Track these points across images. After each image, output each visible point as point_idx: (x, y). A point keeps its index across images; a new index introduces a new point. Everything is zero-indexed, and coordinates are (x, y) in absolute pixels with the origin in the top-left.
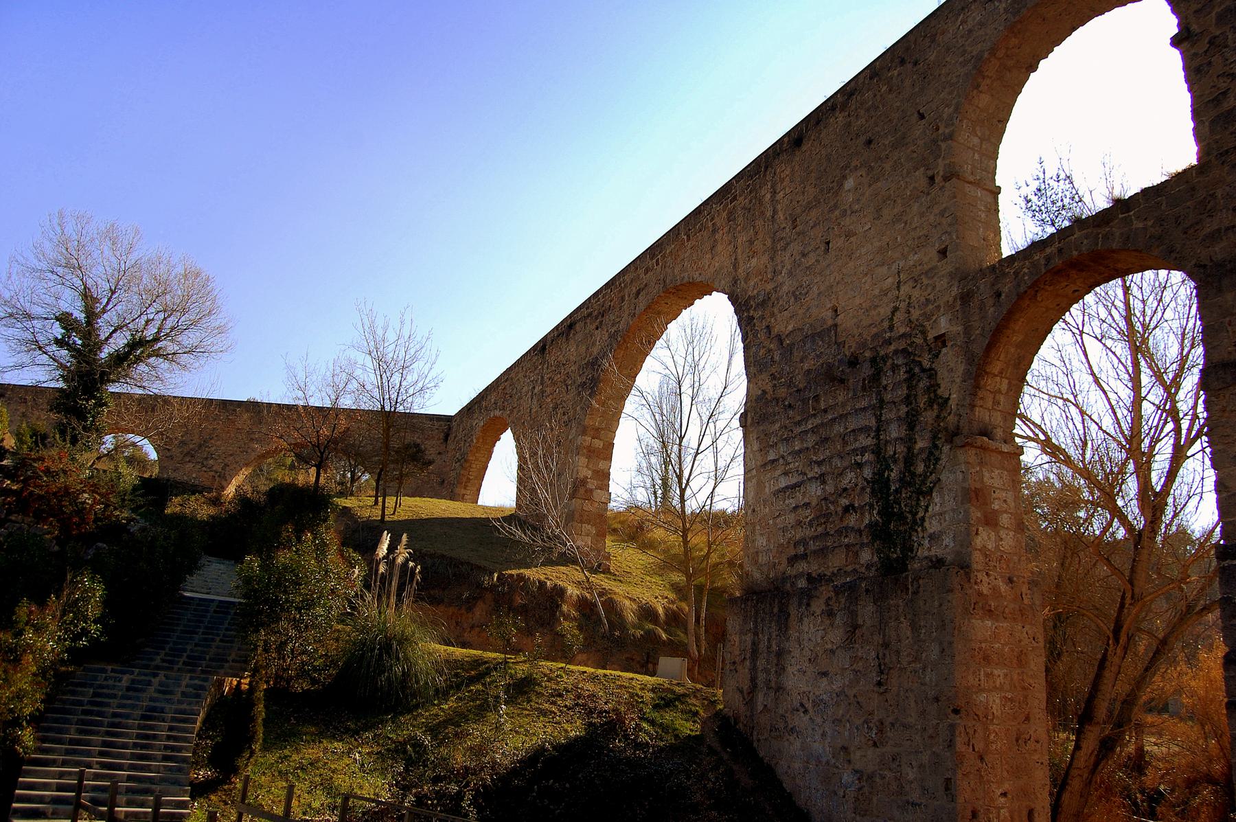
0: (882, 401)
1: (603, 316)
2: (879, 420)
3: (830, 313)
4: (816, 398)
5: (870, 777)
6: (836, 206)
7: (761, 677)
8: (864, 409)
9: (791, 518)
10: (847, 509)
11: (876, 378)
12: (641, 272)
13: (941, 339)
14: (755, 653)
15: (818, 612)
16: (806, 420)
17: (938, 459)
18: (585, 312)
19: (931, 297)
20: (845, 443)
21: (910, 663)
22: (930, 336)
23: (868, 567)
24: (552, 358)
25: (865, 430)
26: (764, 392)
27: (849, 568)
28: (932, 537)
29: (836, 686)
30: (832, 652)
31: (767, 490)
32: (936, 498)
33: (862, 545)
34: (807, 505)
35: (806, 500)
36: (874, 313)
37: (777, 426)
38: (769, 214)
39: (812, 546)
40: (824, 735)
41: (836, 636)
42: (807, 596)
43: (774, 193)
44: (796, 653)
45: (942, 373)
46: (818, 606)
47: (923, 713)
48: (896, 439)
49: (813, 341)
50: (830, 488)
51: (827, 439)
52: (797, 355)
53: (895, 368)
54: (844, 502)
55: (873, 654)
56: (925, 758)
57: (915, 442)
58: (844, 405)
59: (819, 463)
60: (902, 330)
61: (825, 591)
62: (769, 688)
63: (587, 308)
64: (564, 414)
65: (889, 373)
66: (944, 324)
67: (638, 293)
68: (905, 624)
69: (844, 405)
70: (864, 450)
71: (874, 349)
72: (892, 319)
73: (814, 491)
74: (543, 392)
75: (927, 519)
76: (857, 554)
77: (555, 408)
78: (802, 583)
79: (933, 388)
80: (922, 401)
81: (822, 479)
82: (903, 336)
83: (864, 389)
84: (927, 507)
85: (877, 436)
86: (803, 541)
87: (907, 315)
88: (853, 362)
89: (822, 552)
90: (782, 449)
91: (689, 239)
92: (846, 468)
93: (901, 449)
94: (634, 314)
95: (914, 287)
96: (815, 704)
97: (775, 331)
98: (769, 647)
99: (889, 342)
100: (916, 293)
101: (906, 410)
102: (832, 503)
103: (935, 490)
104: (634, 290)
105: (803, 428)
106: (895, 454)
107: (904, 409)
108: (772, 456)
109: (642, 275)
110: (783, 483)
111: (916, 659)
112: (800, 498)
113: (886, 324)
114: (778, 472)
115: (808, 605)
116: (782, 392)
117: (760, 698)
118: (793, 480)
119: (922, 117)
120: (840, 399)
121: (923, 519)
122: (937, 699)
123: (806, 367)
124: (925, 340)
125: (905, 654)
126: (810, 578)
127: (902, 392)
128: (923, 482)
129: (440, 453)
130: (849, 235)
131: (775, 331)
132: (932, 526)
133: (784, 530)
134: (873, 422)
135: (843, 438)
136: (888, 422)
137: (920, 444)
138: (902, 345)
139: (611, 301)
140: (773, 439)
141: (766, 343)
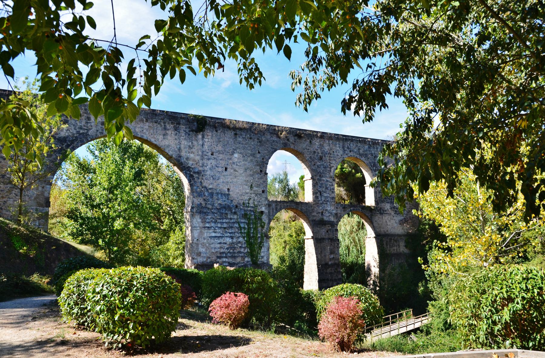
4: (227, 214)
6: (231, 159)
10: (241, 247)
13: (262, 213)
16: (223, 219)
26: (201, 203)
28: (262, 257)
31: (205, 235)
32: (263, 248)
34: (225, 243)
35: (225, 242)
37: (209, 217)
38: (201, 143)
49: (222, 196)
52: (215, 197)
54: (240, 245)
59: (230, 233)
60: (252, 205)
66: (263, 209)
73: (229, 240)
76: (244, 259)
81: (232, 238)
82: (252, 207)
83: (242, 217)
90: (213, 225)
99: (248, 207)
100: (256, 198)
105: (221, 221)
108: (207, 225)
110: (214, 235)
114: (211, 231)
116: (210, 207)
118: (219, 235)
119: (259, 152)
123: (219, 202)
130: (235, 170)
131: (204, 184)
132: (262, 254)
133: (215, 248)
138: (252, 209)
141: (201, 187)
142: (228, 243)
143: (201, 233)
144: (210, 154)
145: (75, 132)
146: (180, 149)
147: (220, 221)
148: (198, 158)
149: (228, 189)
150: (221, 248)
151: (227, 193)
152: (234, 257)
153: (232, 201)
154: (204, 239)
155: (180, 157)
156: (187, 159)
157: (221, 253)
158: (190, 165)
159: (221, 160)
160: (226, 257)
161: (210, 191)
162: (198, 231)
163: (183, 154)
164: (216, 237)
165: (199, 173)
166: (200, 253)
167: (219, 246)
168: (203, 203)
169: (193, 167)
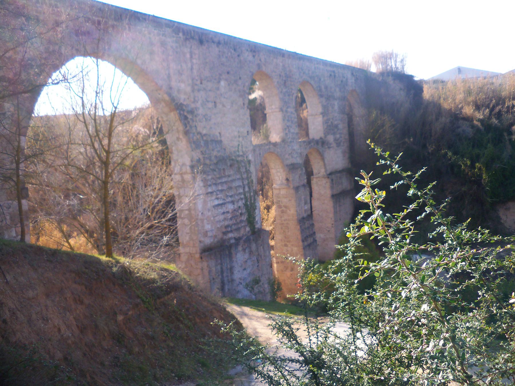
7: (226, 279)
23: (248, 232)
31: (209, 205)
34: (228, 212)
35: (227, 210)
37: (210, 177)
39: (234, 227)
41: (247, 256)
46: (240, 248)
50: (236, 206)
59: (231, 196)
61: (242, 242)
62: (229, 282)
73: (230, 207)
78: (233, 241)
81: (233, 202)
89: (238, 229)
90: (214, 188)
108: (210, 190)
110: (217, 202)
112: (224, 209)
114: (214, 197)
118: (221, 202)
126: (235, 238)
133: (220, 221)
134: (241, 184)
140: (209, 183)
142: (230, 211)
143: (205, 202)
144: (198, 82)
145: (42, 48)
146: (169, 76)
147: (220, 181)
148: (189, 89)
149: (220, 133)
150: (225, 219)
151: (219, 139)
152: (238, 229)
153: (225, 149)
154: (209, 210)
155: (171, 88)
156: (179, 91)
157: (226, 227)
158: (182, 101)
159: (210, 90)
160: (231, 231)
161: (205, 138)
162: (202, 200)
163: (173, 84)
164: (218, 205)
165: (192, 112)
166: (207, 232)
167: (222, 217)
168: (201, 157)
169: (185, 103)
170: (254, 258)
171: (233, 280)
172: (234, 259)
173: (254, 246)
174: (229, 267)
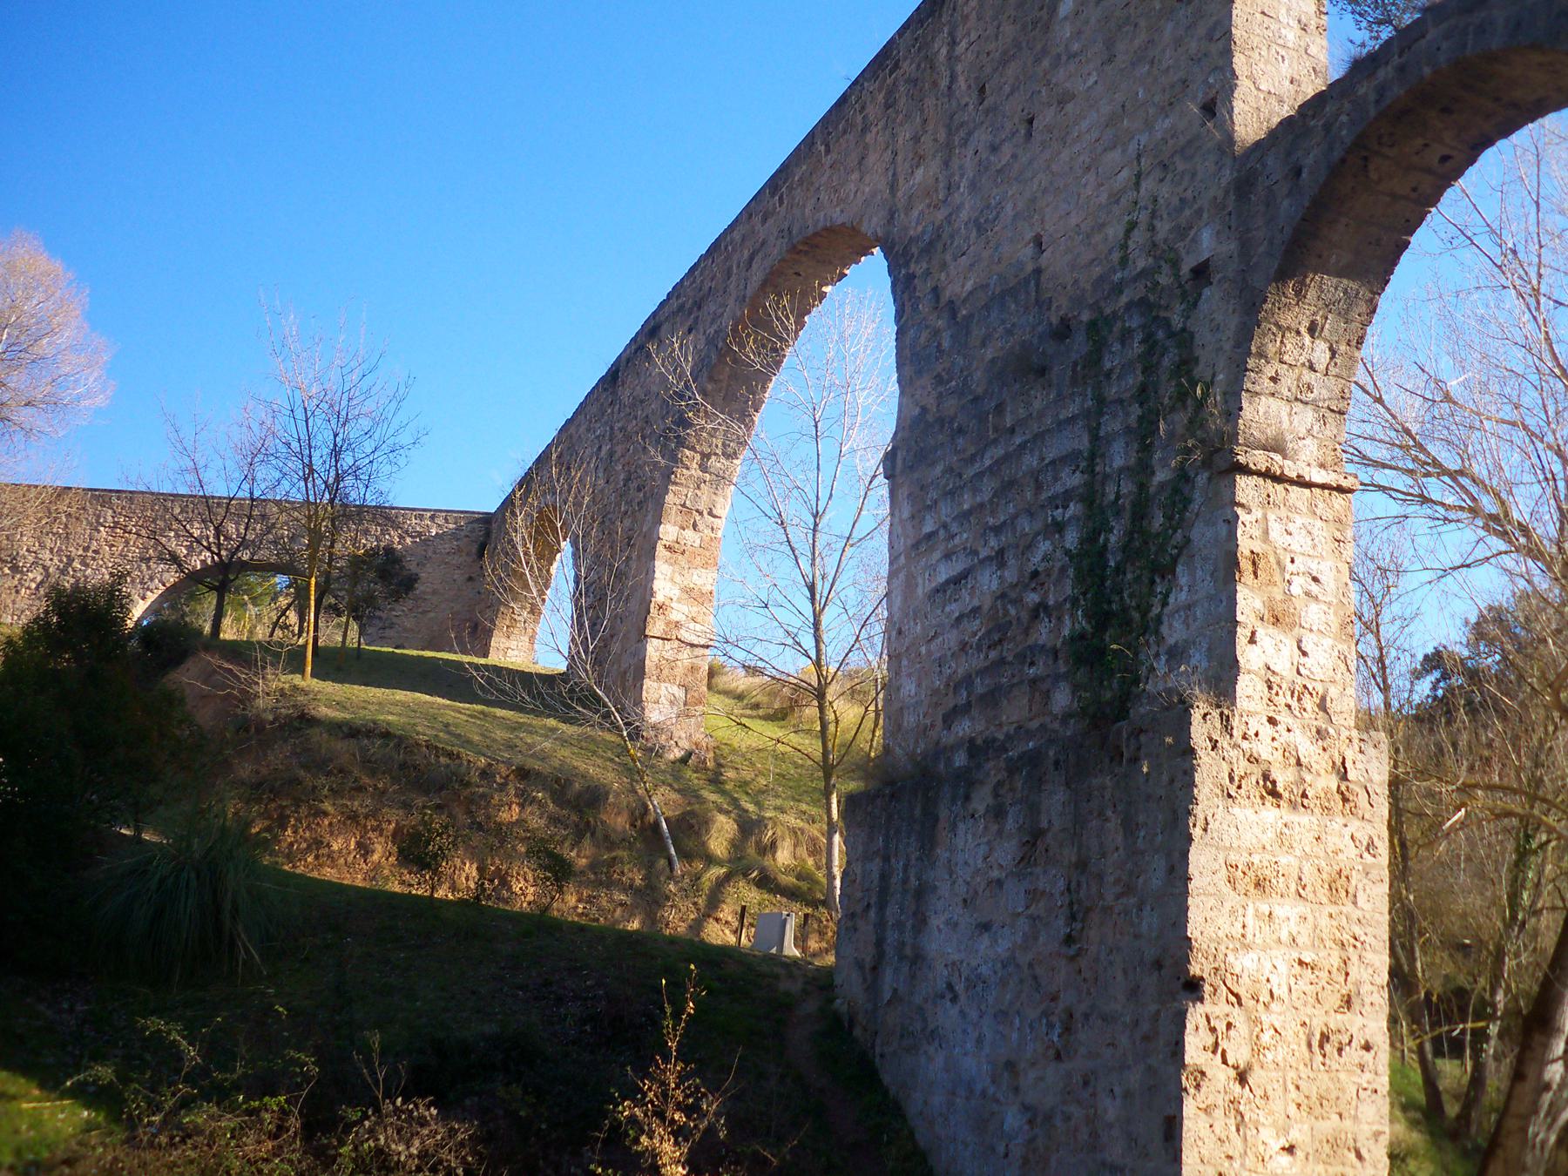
0: (1101, 401)
1: (699, 308)
2: (1095, 438)
3: (1029, 250)
4: (1000, 409)
5: (1048, 1118)
7: (892, 937)
8: (1072, 420)
9: (952, 639)
11: (1094, 359)
12: (757, 219)
14: (884, 891)
15: (981, 809)
16: (981, 453)
17: (1187, 501)
18: (675, 304)
19: (1189, 194)
20: (1039, 487)
21: (1118, 897)
22: (1185, 269)
23: (1066, 717)
24: (625, 394)
25: (1070, 458)
27: (1034, 724)
29: (1003, 946)
30: (999, 883)
33: (1057, 678)
34: (976, 611)
35: (976, 603)
36: (1097, 238)
37: (939, 469)
39: (980, 687)
40: (980, 1041)
41: (1007, 852)
42: (966, 782)
43: (953, 43)
44: (944, 888)
45: (1203, 335)
46: (982, 800)
47: (1134, 993)
48: (1121, 470)
50: (1011, 575)
51: (1012, 483)
52: (977, 332)
53: (1125, 336)
54: (1032, 598)
55: (1061, 884)
56: (1135, 1078)
57: (1153, 473)
58: (1041, 415)
59: (997, 530)
61: (993, 770)
62: (902, 958)
63: (678, 297)
64: (639, 490)
65: (1116, 347)
66: (1207, 243)
67: (751, 258)
68: (1114, 823)
69: (1041, 415)
70: (1067, 497)
71: (1095, 307)
72: (1124, 246)
73: (988, 582)
74: (611, 454)
75: (1165, 619)
76: (1047, 695)
77: (627, 480)
78: (960, 759)
79: (1186, 365)
80: (1167, 392)
81: (999, 558)
82: (1143, 273)
83: (1074, 382)
84: (1167, 596)
85: (1091, 470)
86: (968, 680)
87: (1149, 234)
88: (1063, 331)
89: (991, 699)
91: (828, 151)
92: (1038, 534)
93: (1127, 487)
94: (744, 297)
95: (1162, 180)
96: (970, 985)
97: (947, 295)
98: (905, 881)
99: (1118, 289)
100: (1165, 191)
101: (1139, 412)
102: (1014, 602)
103: (1181, 560)
104: (746, 253)
105: (977, 467)
106: (1118, 497)
107: (1136, 410)
109: (758, 227)
110: (944, 573)
111: (1129, 890)
112: (967, 600)
113: (1116, 256)
114: (937, 555)
115: (967, 798)
117: (888, 979)
118: (956, 567)
120: (1037, 405)
121: (1159, 620)
122: (1158, 965)
124: (1177, 276)
125: (1111, 879)
127: (1134, 380)
128: (1162, 549)
129: (470, 579)
131: (947, 295)
134: (1084, 443)
135: (1035, 475)
136: (1110, 439)
137: (1161, 476)
139: (712, 280)
140: (933, 494)
149: (1038, 242)
170: (1052, 880)
171: (917, 959)
172: (942, 853)
173: (1055, 802)
174: (914, 882)
